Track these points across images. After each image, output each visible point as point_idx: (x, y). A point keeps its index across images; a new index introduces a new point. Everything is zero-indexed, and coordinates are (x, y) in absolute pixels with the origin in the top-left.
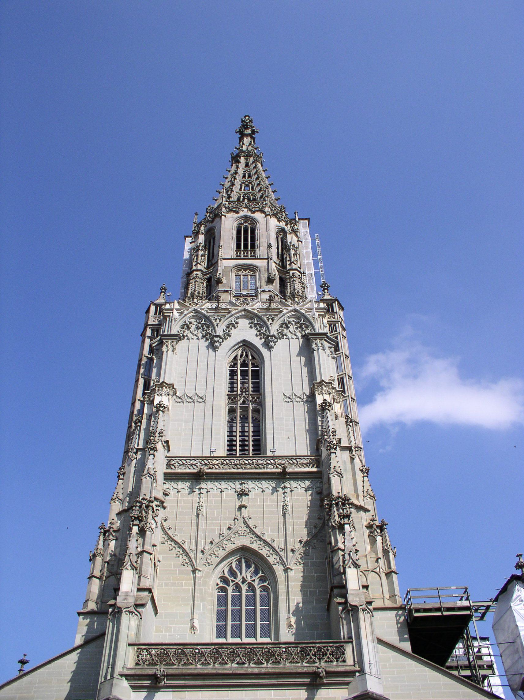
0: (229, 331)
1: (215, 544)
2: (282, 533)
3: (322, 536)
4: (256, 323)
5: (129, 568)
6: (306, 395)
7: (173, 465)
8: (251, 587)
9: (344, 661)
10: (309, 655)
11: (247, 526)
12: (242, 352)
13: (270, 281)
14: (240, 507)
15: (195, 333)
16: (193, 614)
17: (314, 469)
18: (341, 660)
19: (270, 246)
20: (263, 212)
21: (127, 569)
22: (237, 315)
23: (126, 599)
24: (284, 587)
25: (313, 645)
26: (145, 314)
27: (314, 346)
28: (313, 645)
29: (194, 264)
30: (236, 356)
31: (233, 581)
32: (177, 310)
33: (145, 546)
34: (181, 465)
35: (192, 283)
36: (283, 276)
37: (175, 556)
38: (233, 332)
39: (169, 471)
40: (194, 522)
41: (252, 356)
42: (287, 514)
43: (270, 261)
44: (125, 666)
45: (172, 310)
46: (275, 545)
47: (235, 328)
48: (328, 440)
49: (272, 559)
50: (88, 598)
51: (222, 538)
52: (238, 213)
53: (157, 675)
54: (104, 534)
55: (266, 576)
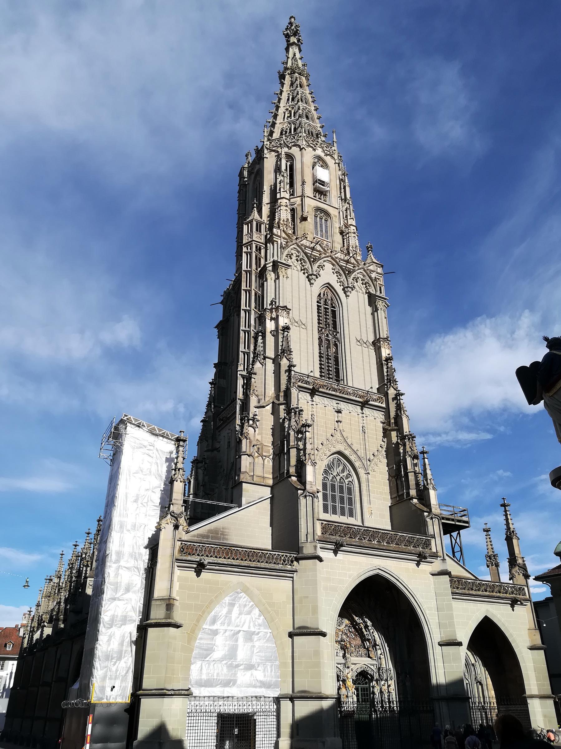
0: (319, 271)
5: (310, 464)
9: (431, 549)
12: (324, 292)
30: (320, 294)
46: (359, 453)
52: (314, 150)
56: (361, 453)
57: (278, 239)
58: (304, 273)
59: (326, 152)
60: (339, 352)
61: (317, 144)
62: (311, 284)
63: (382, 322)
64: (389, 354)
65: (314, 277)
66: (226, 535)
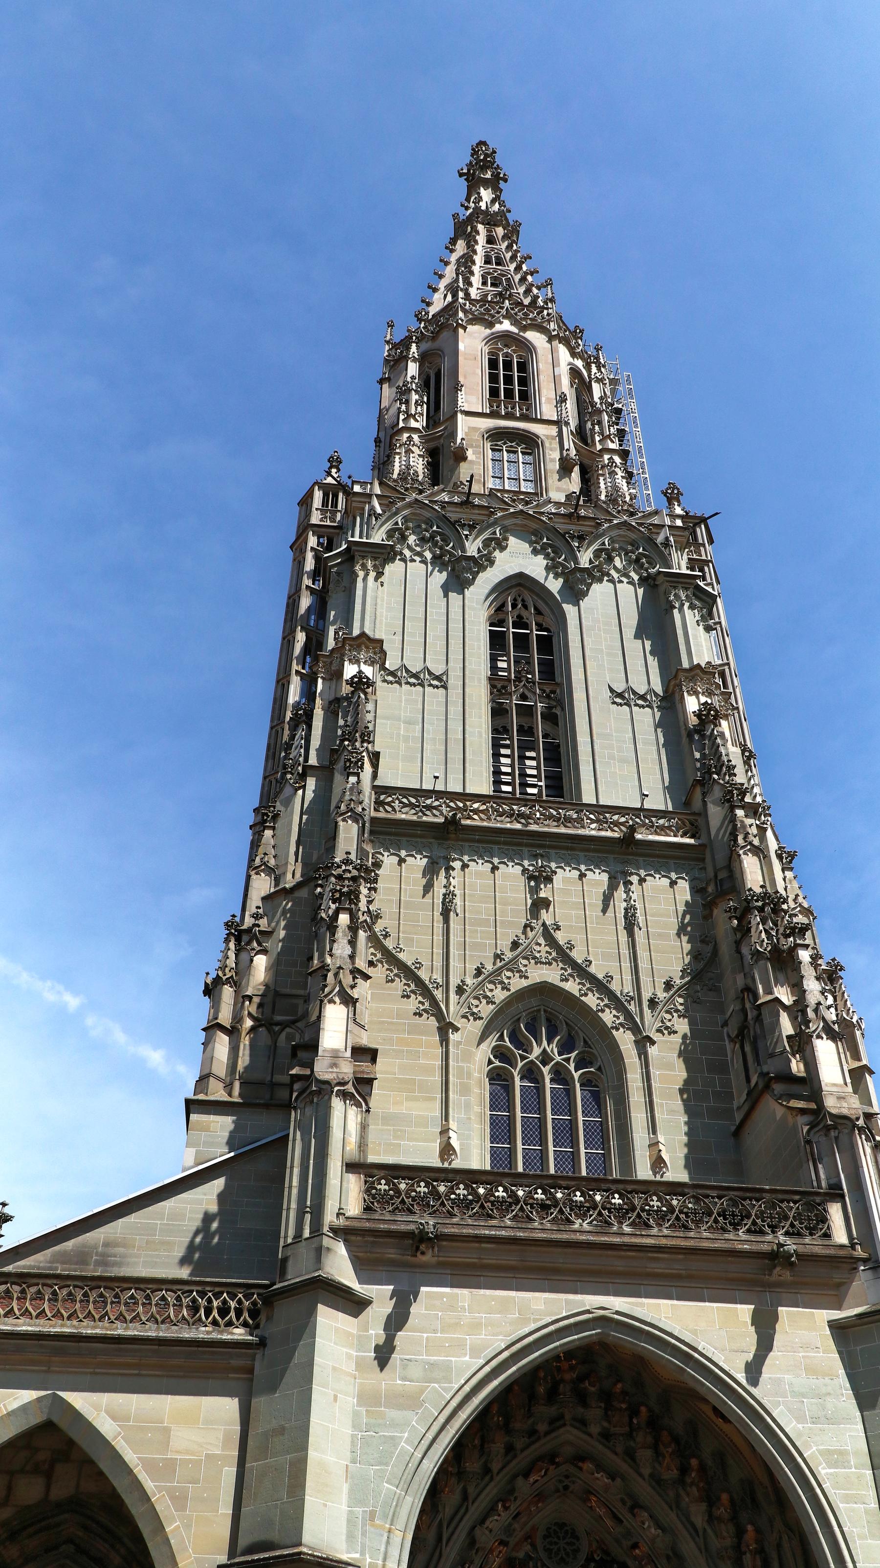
0: (490, 553)
1: (487, 973)
2: (626, 965)
3: (711, 979)
4: (544, 543)
5: (337, 999)
6: (656, 695)
7: (389, 804)
8: (560, 1075)
9: (827, 1235)
10: (748, 1216)
11: (551, 941)
12: (515, 600)
13: (565, 468)
14: (539, 905)
15: (418, 549)
16: (447, 1119)
17: (691, 841)
18: (820, 1233)
19: (562, 399)
21: (332, 1001)
22: (507, 522)
23: (334, 1065)
24: (638, 1076)
25: (757, 1195)
26: (298, 508)
27: (672, 598)
28: (757, 1195)
29: (402, 417)
31: (523, 1058)
32: (377, 496)
33: (357, 961)
34: (405, 805)
35: (399, 454)
36: (586, 462)
37: (400, 993)
39: (382, 815)
40: (439, 925)
41: (536, 609)
42: (636, 929)
43: (564, 429)
44: (341, 1211)
45: (370, 496)
46: (615, 986)
48: (721, 781)
49: (608, 1017)
50: (206, 1072)
51: (499, 964)
52: (491, 325)
53: (428, 1233)
54: (238, 940)
55: (596, 1053)
56: (622, 985)
66: (115, 1264)
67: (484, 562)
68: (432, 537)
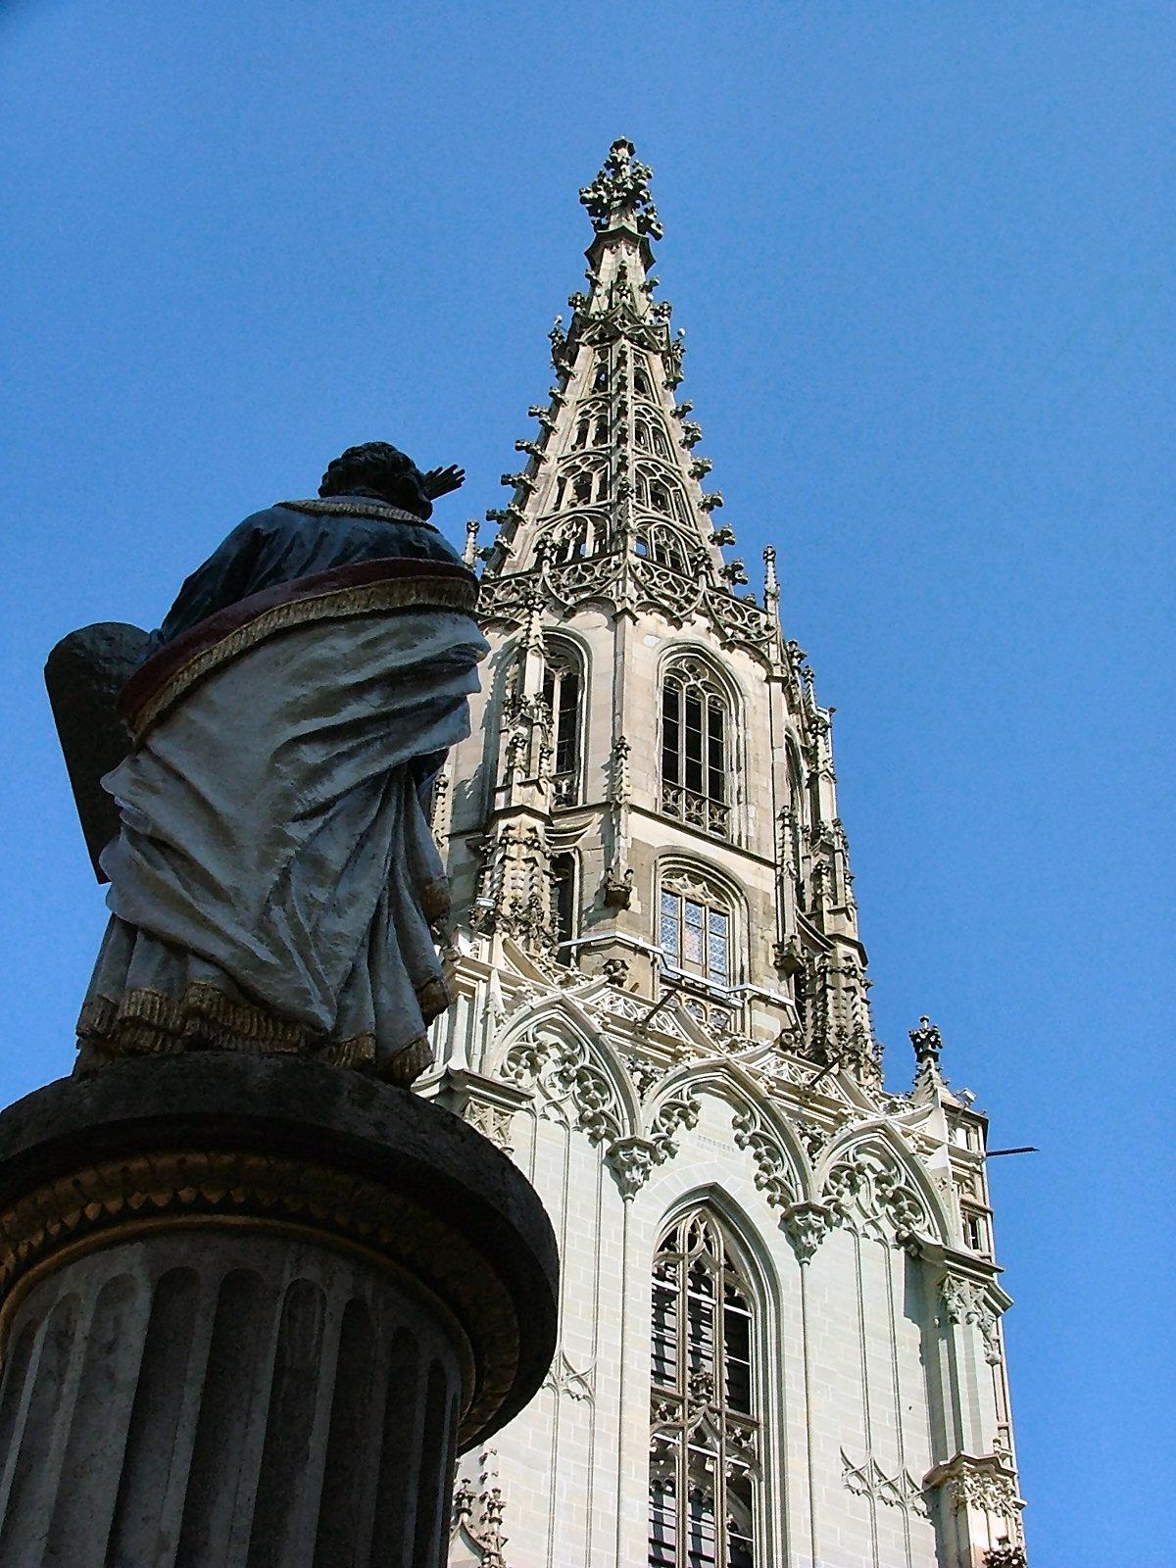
0: (670, 1132)
12: (693, 1228)
15: (556, 1097)
20: (761, 659)
30: (673, 1236)
38: (681, 1136)
47: (689, 1127)
52: (677, 623)
57: (478, 979)
58: (595, 1138)
59: (729, 631)
60: (758, 1522)
61: (689, 601)
62: (628, 1189)
63: (972, 1381)
64: (1004, 1540)
65: (643, 1157)
67: (662, 1148)
68: (580, 1078)
